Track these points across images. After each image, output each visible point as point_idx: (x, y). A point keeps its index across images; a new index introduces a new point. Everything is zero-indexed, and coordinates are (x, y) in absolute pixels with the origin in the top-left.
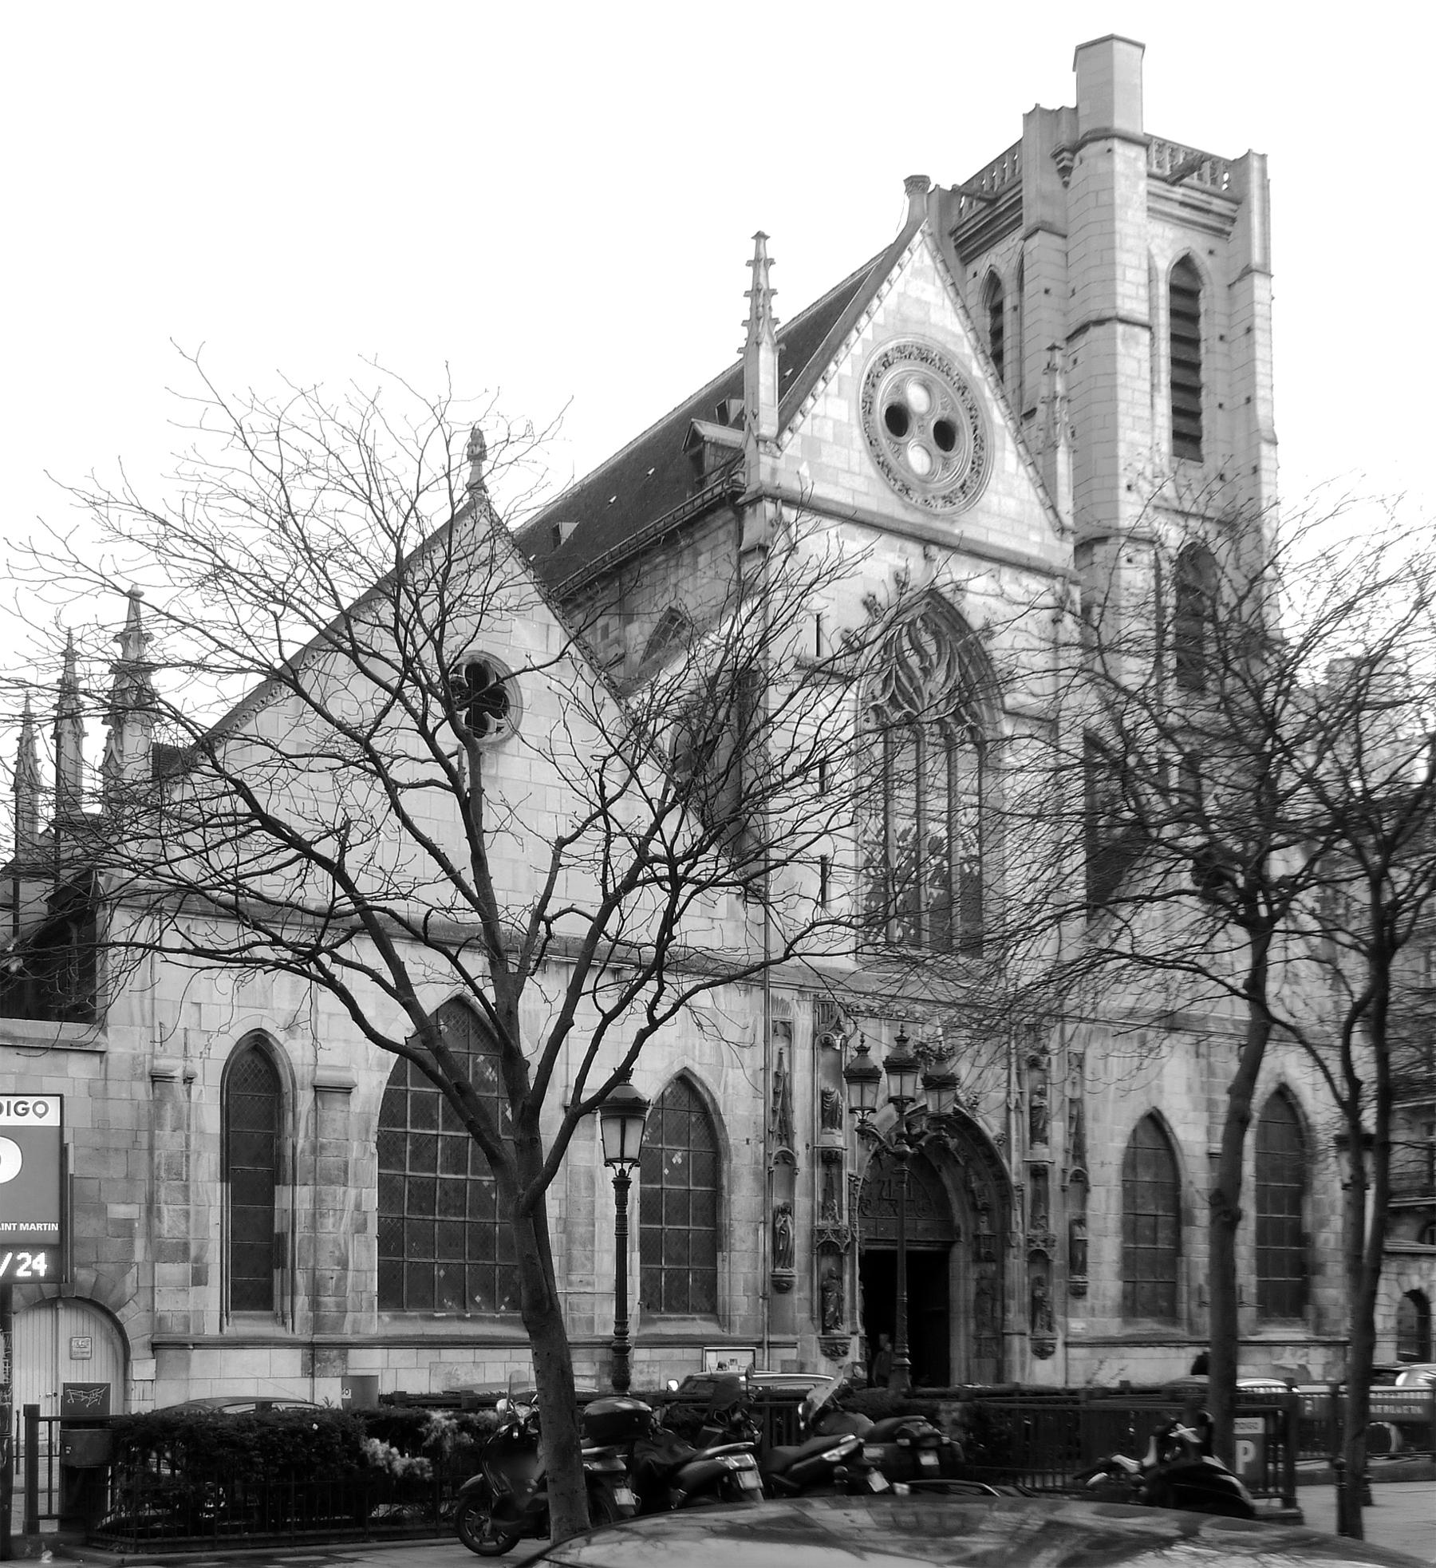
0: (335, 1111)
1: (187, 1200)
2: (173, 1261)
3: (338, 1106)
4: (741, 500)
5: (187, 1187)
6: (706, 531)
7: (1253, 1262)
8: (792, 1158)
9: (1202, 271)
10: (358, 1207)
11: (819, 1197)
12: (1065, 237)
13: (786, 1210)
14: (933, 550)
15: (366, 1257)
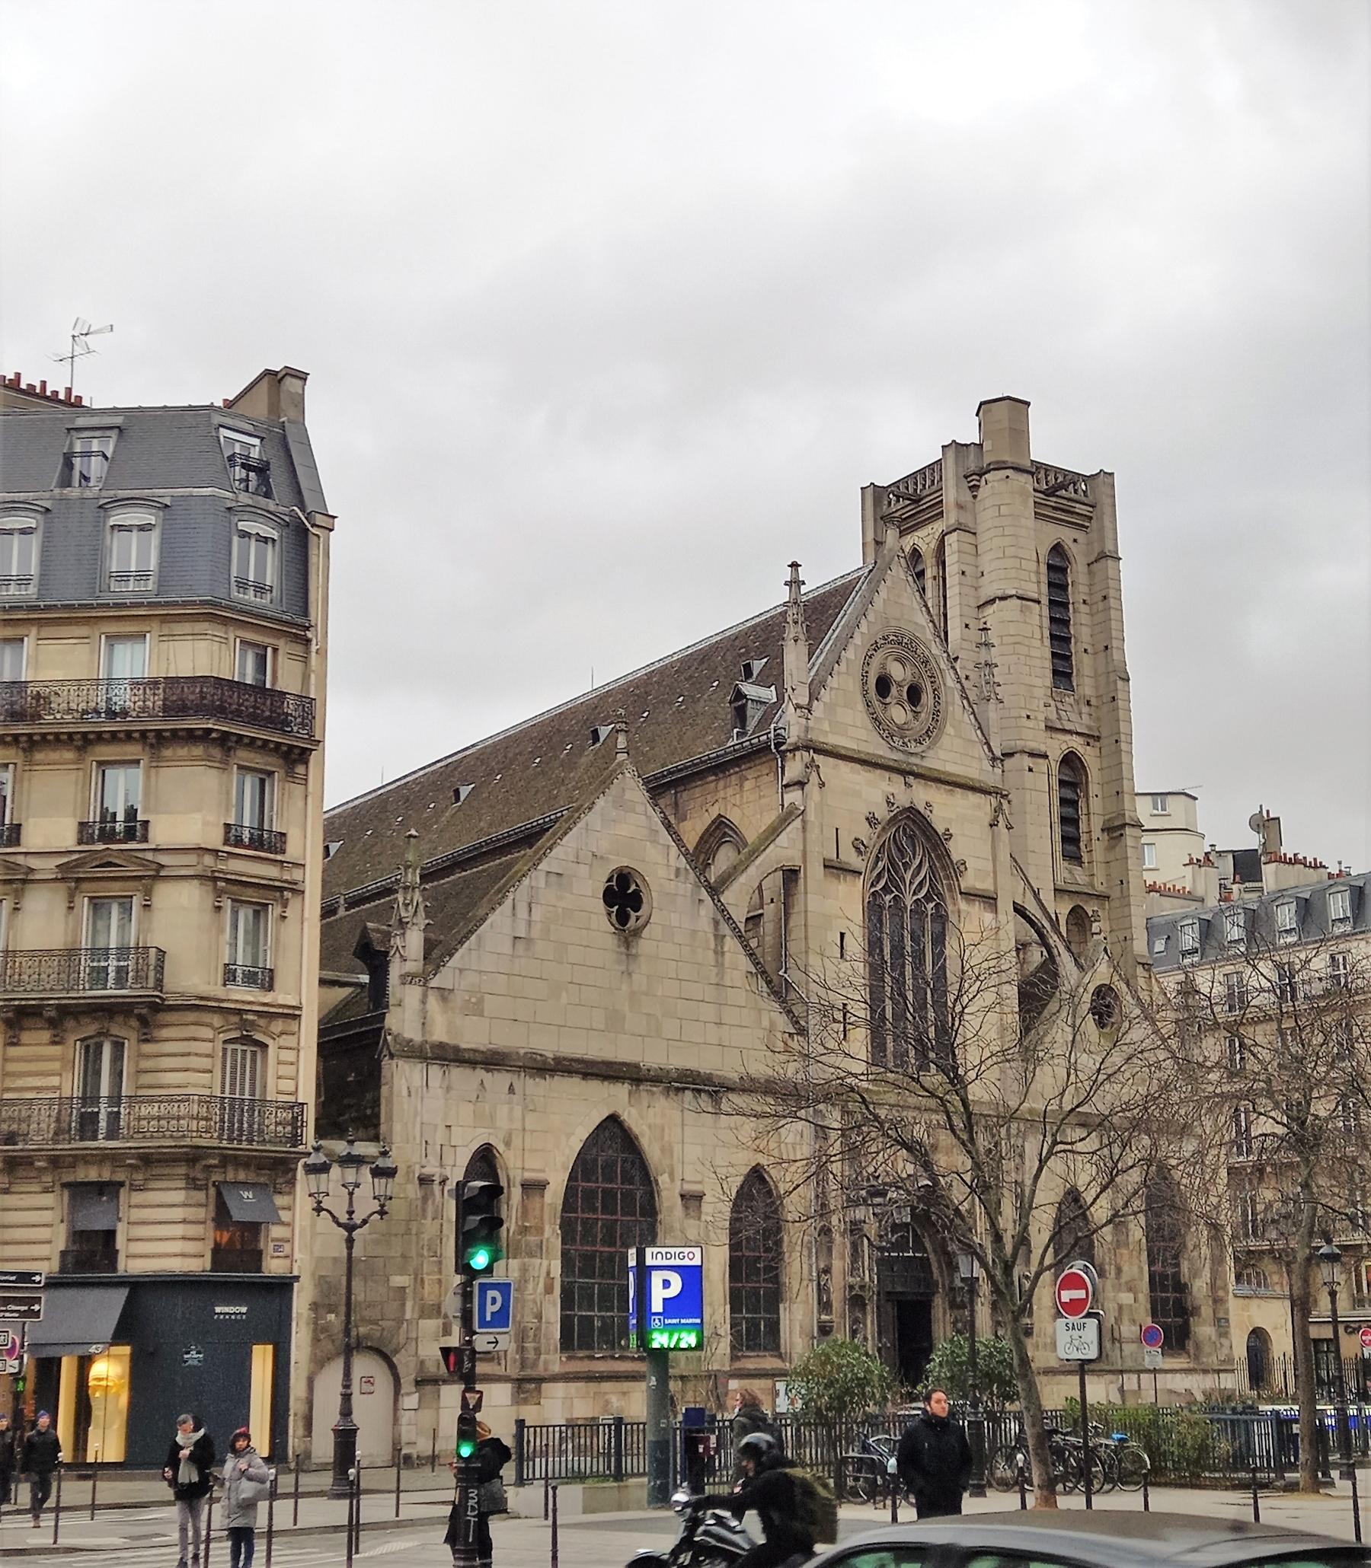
0: (535, 1202)
1: (440, 1272)
2: (430, 1318)
3: (537, 1199)
4: (783, 748)
5: (440, 1263)
6: (752, 764)
7: (1149, 1306)
8: (830, 1230)
9: (1070, 555)
10: (548, 1273)
11: (848, 1260)
12: (975, 534)
13: (827, 1271)
14: (911, 779)
15: (553, 1313)
